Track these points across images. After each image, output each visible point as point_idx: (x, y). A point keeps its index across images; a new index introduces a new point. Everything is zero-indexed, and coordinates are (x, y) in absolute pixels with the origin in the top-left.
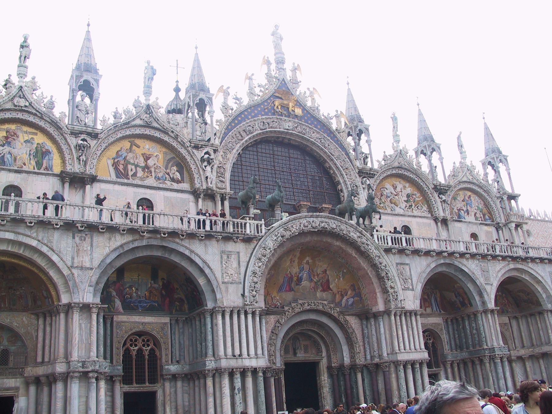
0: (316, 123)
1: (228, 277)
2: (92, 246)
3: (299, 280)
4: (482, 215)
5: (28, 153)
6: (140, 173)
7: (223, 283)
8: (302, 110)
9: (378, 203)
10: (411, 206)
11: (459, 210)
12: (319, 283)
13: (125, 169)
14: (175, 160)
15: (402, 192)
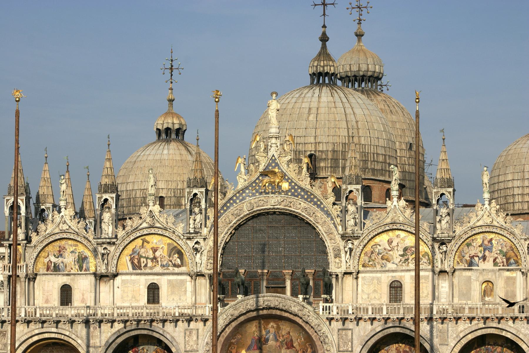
0: (303, 193)
1: (189, 347)
2: (100, 332)
3: (267, 340)
4: (505, 260)
5: (73, 260)
6: (150, 264)
7: (185, 351)
8: (290, 183)
9: (367, 262)
10: (408, 259)
11: (472, 257)
12: (284, 342)
13: (139, 262)
14: (176, 249)
15: (398, 246)
